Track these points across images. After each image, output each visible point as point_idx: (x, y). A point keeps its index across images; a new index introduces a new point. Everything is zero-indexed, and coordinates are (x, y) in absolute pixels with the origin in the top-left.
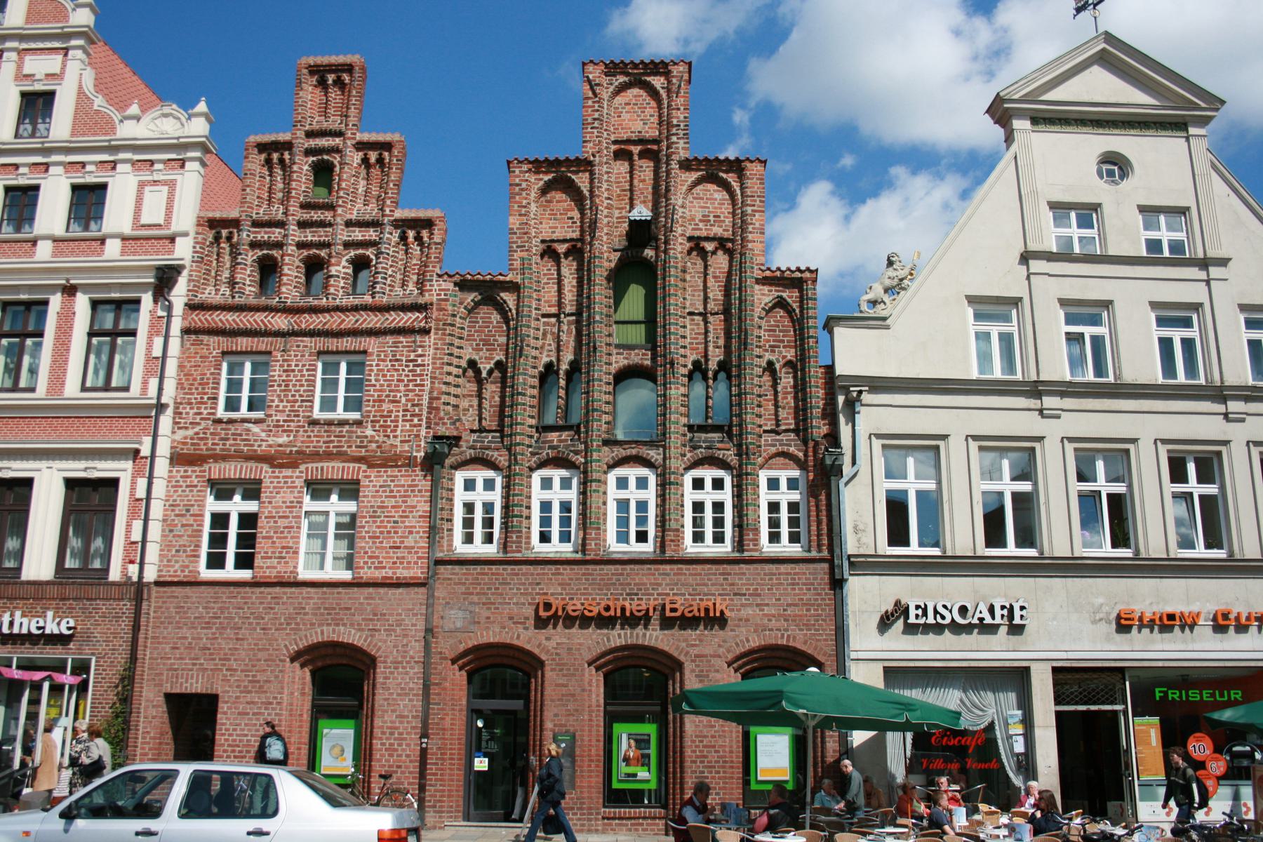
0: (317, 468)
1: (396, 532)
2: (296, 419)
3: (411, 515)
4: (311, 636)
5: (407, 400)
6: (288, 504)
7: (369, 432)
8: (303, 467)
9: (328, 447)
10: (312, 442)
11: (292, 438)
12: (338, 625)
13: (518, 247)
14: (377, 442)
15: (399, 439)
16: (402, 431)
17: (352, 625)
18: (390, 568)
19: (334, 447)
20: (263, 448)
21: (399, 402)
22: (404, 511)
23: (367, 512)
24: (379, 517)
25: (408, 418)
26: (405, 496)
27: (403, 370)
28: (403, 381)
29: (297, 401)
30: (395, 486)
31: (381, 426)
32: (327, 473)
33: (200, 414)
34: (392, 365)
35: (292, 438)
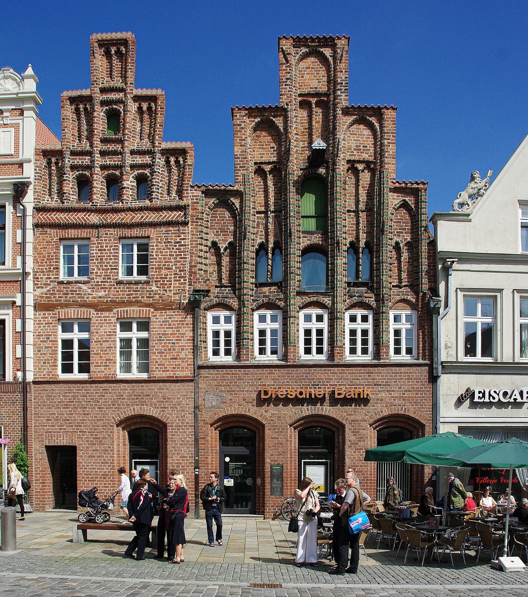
0: (124, 311)
1: (174, 350)
2: (109, 280)
4: (128, 412)
6: (108, 333)
7: (154, 288)
8: (115, 311)
9: (130, 298)
10: (120, 295)
11: (107, 292)
12: (143, 405)
13: (240, 167)
14: (159, 294)
17: (151, 405)
18: (172, 371)
19: (133, 298)
20: (90, 299)
21: (171, 269)
23: (156, 338)
24: (163, 340)
25: (178, 279)
26: (178, 328)
27: (173, 249)
29: (109, 269)
31: (161, 284)
32: (130, 314)
33: (50, 278)
35: (107, 292)
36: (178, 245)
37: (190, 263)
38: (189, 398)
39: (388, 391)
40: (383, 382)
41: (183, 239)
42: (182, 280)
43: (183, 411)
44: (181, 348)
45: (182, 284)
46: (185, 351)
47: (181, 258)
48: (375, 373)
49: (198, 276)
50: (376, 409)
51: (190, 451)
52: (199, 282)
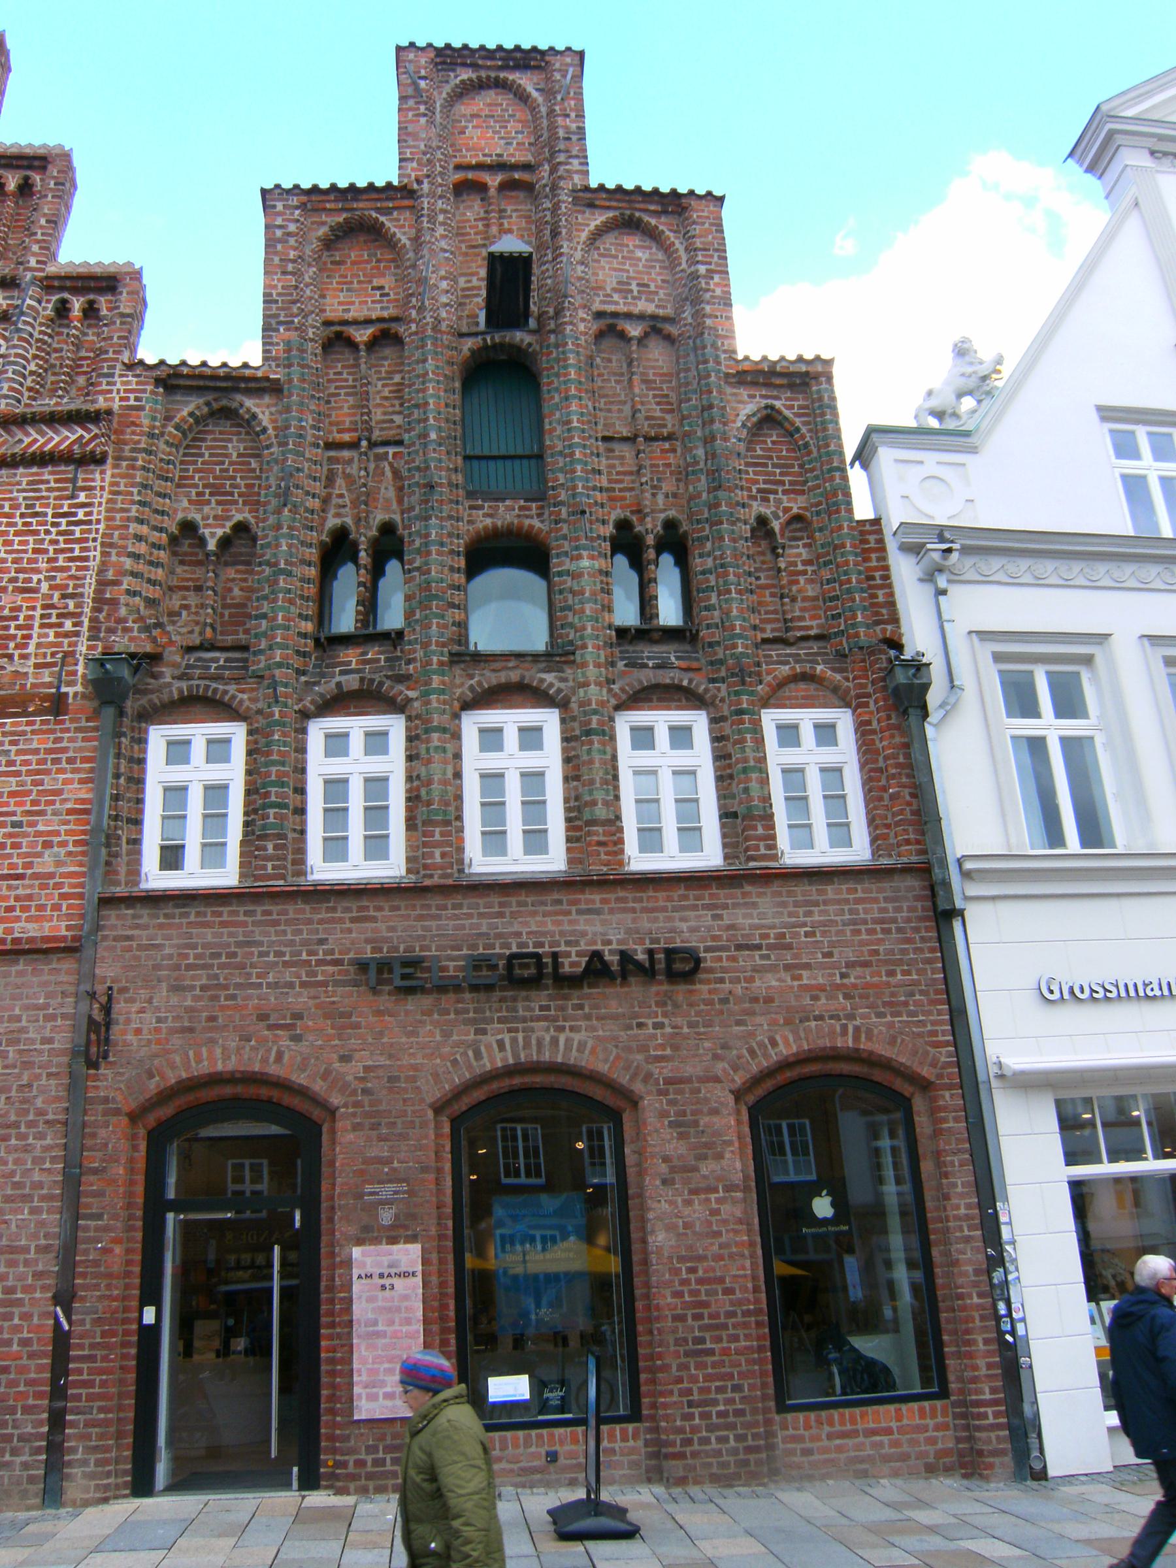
1: (15, 846)
3: (49, 809)
5: (51, 588)
15: (32, 661)
16: (39, 645)
22: (34, 803)
25: (54, 620)
26: (38, 772)
27: (47, 532)
28: (46, 551)
30: (18, 752)
34: (25, 524)
36: (64, 521)
37: (101, 572)
38: (53, 1017)
39: (787, 968)
40: (767, 936)
41: (83, 505)
42: (68, 625)
43: (27, 1065)
44: (41, 839)
45: (67, 635)
46: (56, 849)
47: (71, 559)
48: (735, 905)
49: (123, 611)
50: (752, 1034)
51: (42, 1224)
52: (126, 630)
